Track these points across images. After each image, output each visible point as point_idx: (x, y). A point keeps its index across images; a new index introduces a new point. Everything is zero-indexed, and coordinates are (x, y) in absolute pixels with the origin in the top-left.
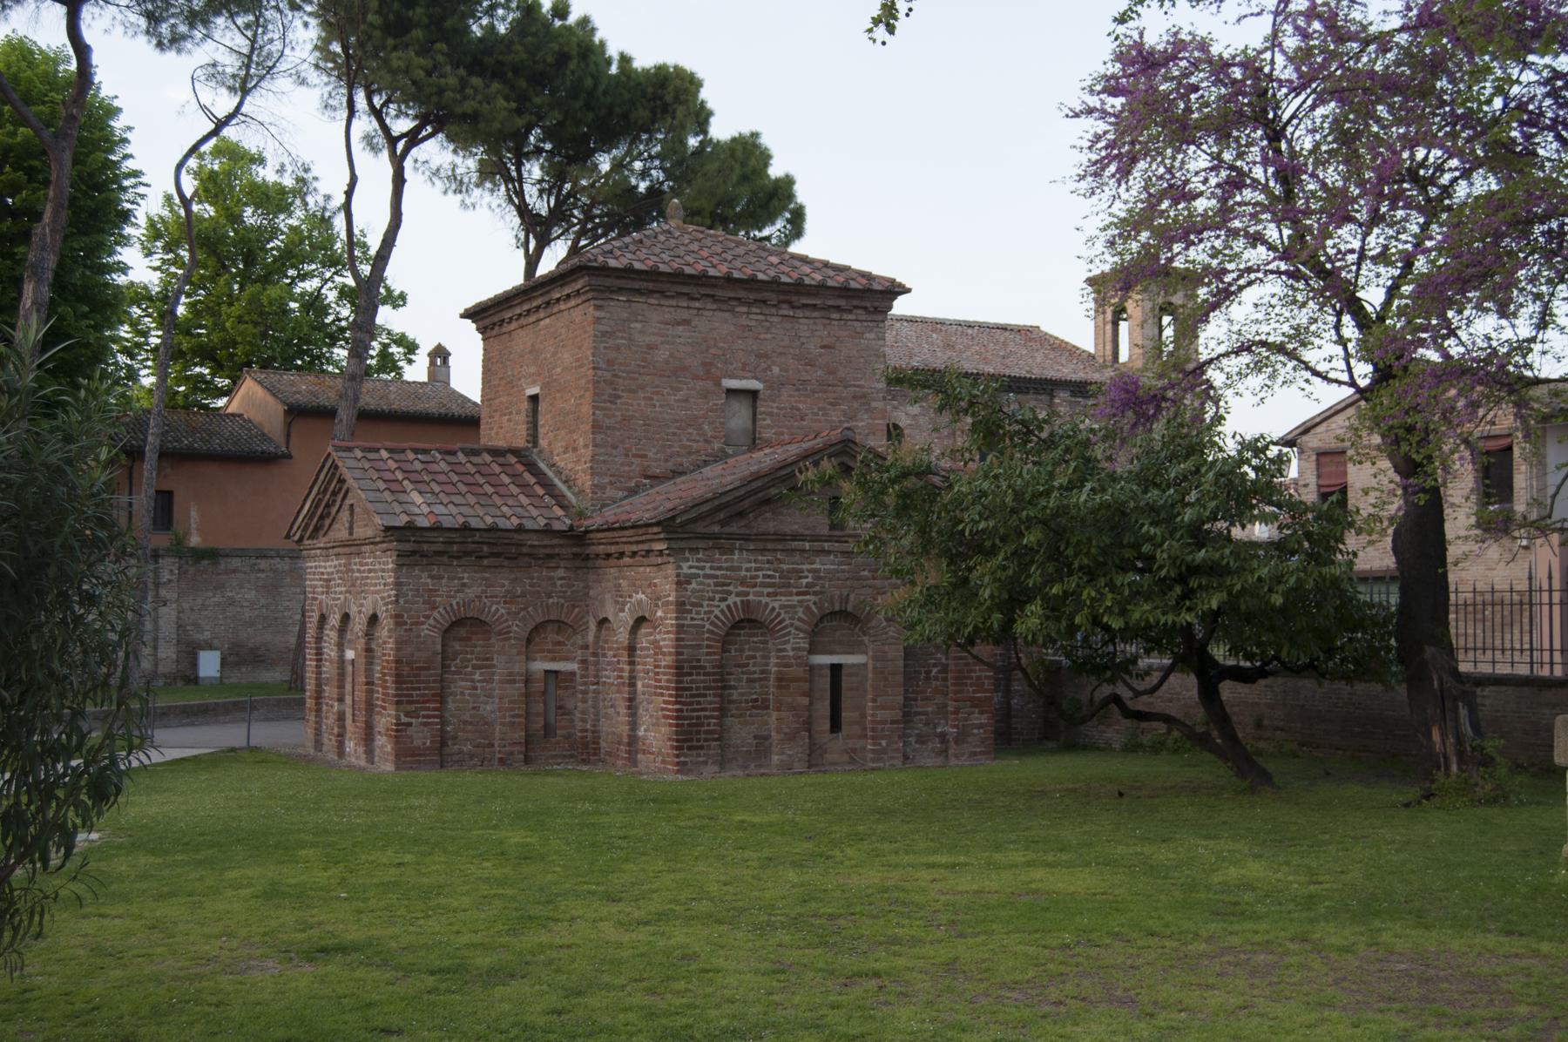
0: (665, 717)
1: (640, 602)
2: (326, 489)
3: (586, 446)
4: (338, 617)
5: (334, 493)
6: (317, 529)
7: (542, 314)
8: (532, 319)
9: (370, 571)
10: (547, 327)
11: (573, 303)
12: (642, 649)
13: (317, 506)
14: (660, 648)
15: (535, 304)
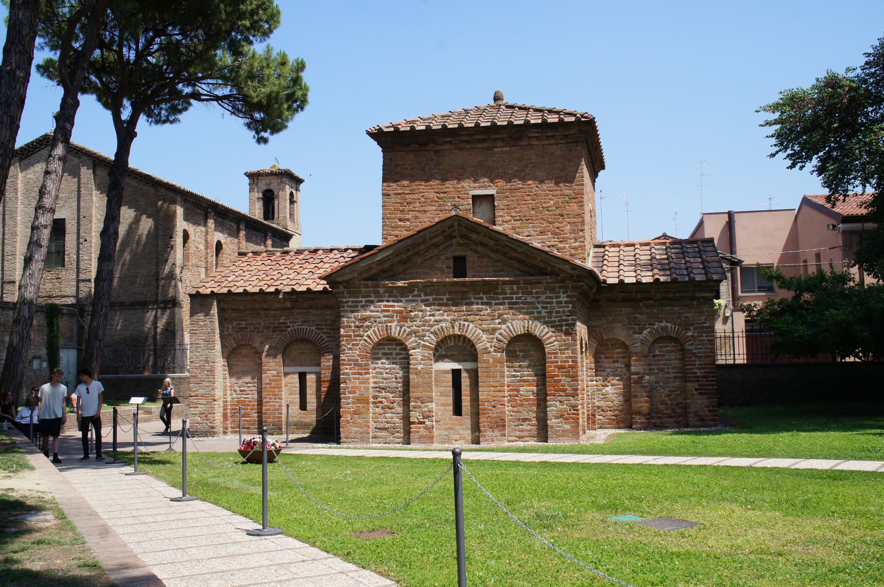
0: (700, 394)
1: (662, 328)
2: (424, 242)
3: (573, 232)
4: (431, 340)
5: (436, 246)
6: (383, 271)
7: (499, 144)
8: (480, 146)
9: (515, 303)
10: (503, 152)
11: (553, 142)
12: (654, 356)
13: (397, 255)
14: (694, 354)
15: (497, 136)
